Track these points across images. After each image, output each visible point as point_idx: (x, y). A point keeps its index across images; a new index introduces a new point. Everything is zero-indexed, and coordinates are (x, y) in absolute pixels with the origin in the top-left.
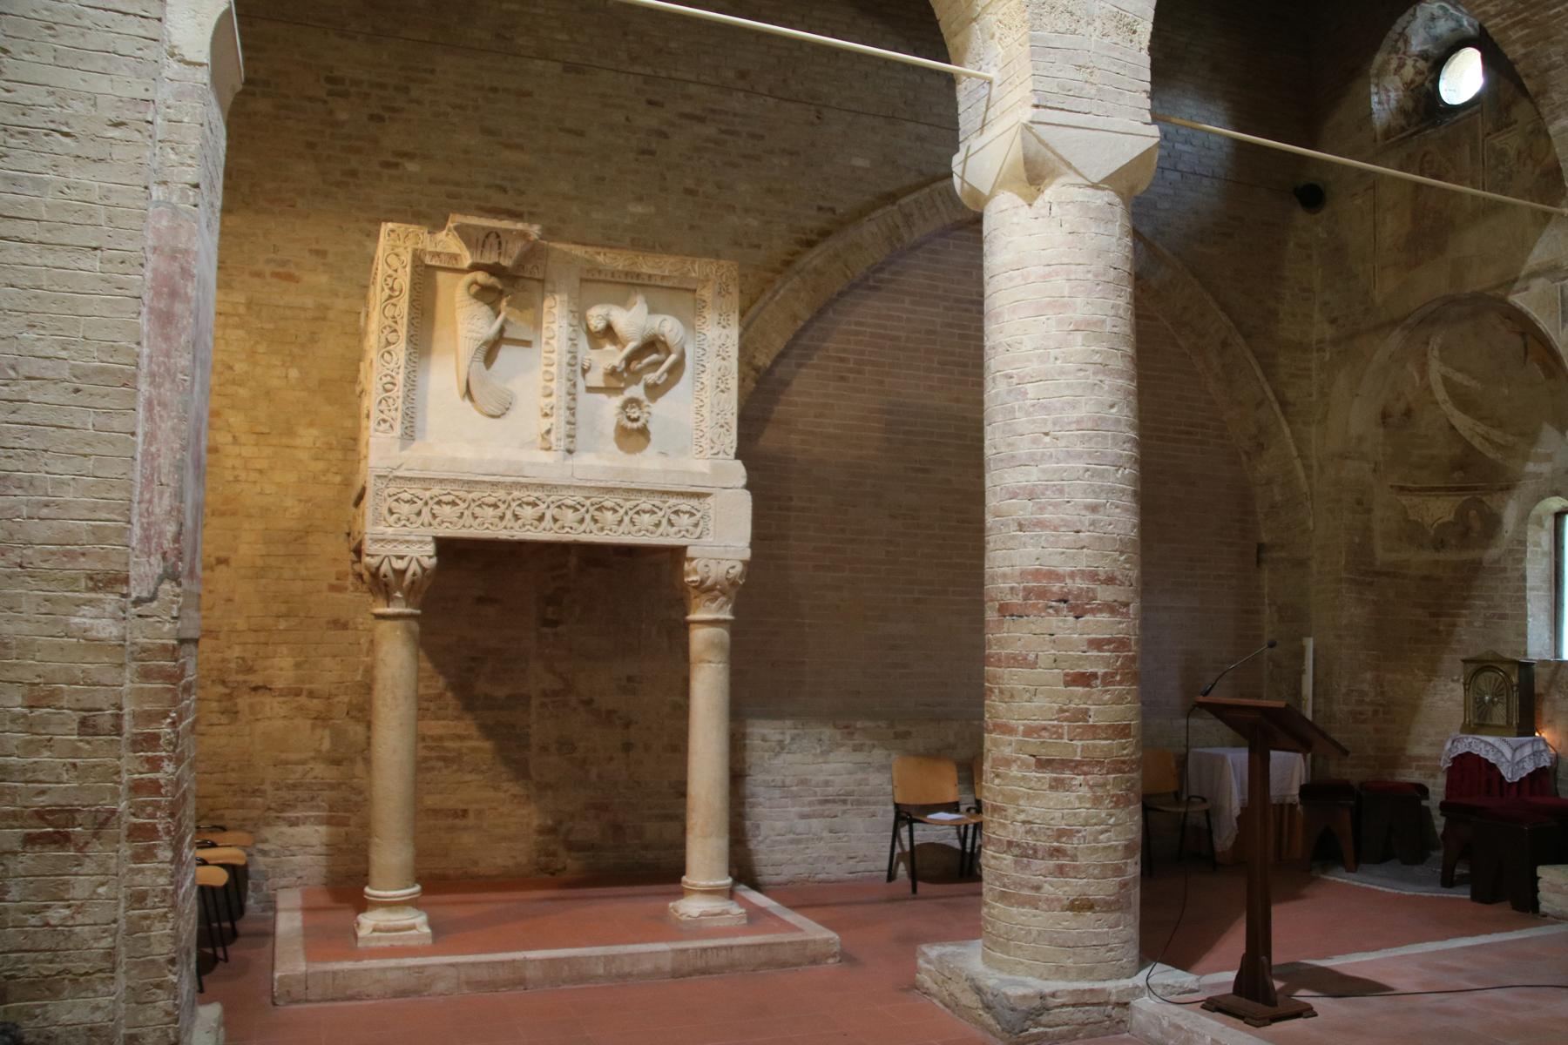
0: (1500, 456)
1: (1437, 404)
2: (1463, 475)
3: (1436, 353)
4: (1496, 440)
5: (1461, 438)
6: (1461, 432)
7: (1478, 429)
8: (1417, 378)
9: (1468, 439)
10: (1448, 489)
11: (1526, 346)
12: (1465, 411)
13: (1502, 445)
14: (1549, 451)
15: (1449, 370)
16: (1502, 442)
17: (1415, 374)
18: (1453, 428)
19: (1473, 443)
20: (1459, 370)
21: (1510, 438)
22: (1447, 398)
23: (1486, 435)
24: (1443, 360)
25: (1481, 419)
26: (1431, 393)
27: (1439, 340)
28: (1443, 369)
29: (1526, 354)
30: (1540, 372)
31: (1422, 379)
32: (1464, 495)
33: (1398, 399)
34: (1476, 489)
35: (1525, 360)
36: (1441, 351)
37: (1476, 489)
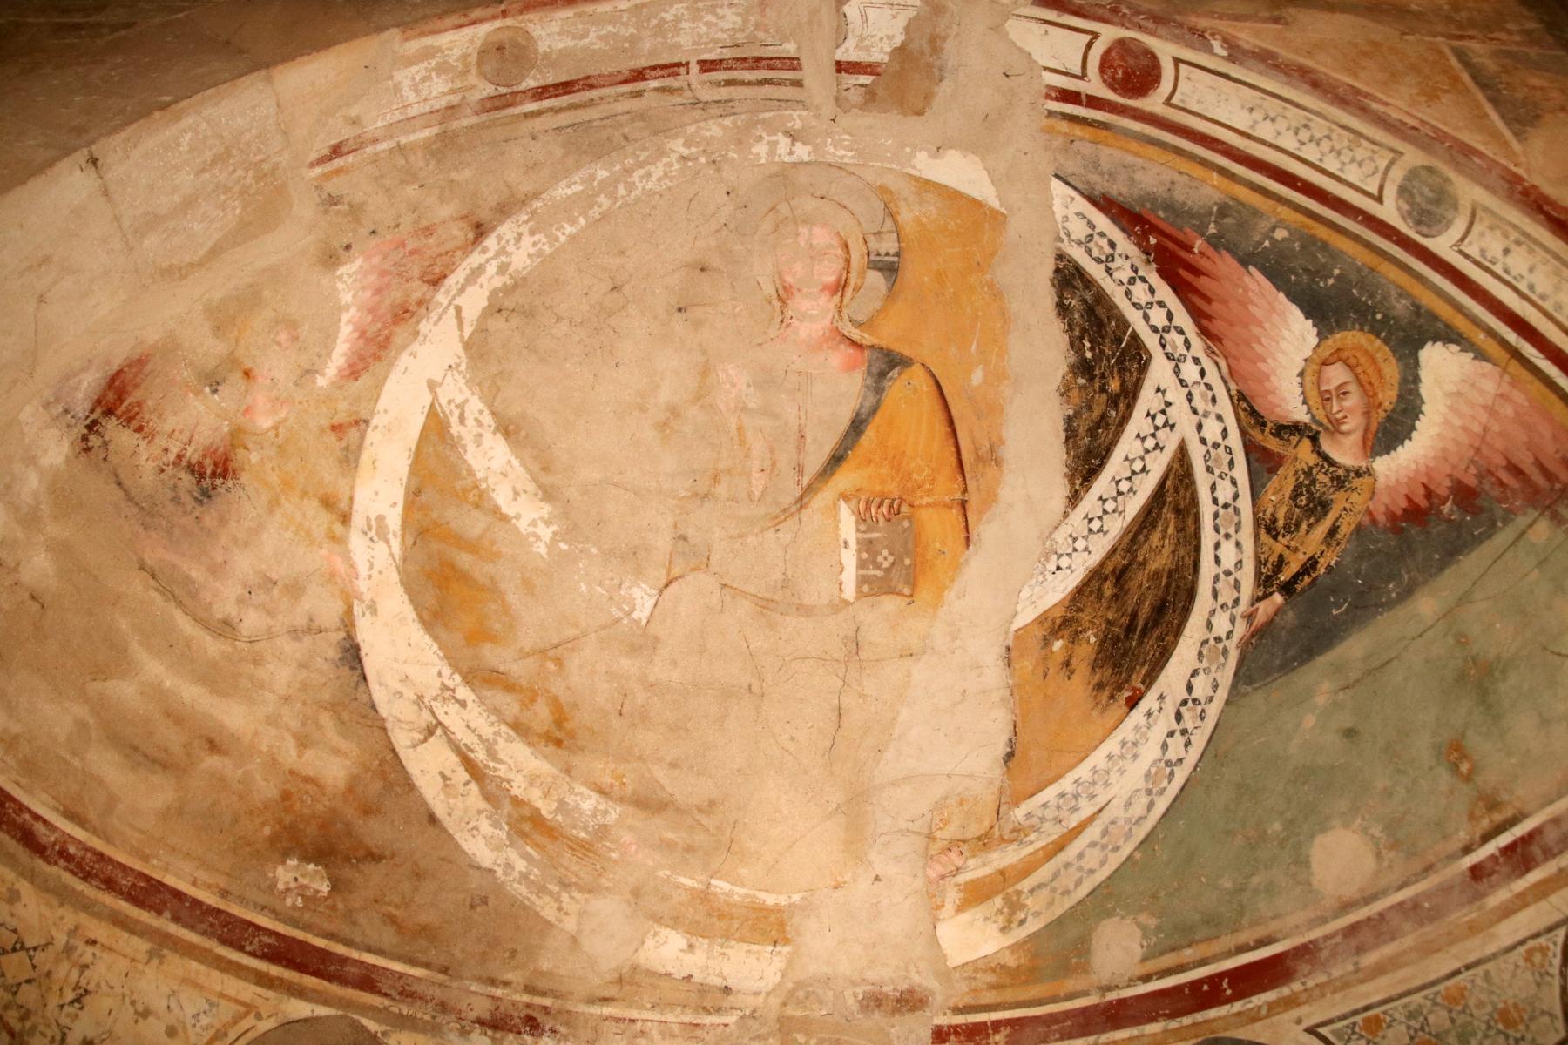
0: (521, 865)
1: (345, 519)
2: (324, 888)
3: (475, 302)
4: (518, 788)
5: (369, 719)
6: (379, 695)
7: (451, 716)
8: (338, 358)
9: (401, 739)
10: (233, 932)
11: (857, 426)
12: (433, 619)
13: (537, 820)
14: (770, 900)
15: (475, 405)
16: (546, 809)
17: (346, 331)
18: (352, 655)
19: (413, 768)
20: (507, 429)
21: (589, 802)
22: (394, 521)
23: (480, 755)
24: (477, 348)
25: (482, 678)
26: (349, 459)
27: (520, 259)
28: (455, 391)
29: (837, 459)
30: (849, 559)
31: (353, 371)
32: (300, 993)
33: (213, 381)
34: (368, 981)
35: (809, 490)
36: (495, 308)
37: (368, 981)
